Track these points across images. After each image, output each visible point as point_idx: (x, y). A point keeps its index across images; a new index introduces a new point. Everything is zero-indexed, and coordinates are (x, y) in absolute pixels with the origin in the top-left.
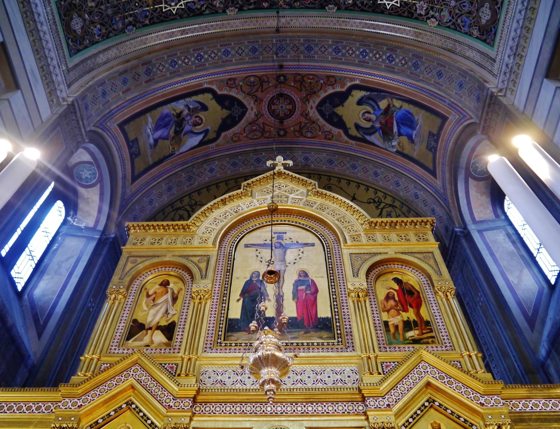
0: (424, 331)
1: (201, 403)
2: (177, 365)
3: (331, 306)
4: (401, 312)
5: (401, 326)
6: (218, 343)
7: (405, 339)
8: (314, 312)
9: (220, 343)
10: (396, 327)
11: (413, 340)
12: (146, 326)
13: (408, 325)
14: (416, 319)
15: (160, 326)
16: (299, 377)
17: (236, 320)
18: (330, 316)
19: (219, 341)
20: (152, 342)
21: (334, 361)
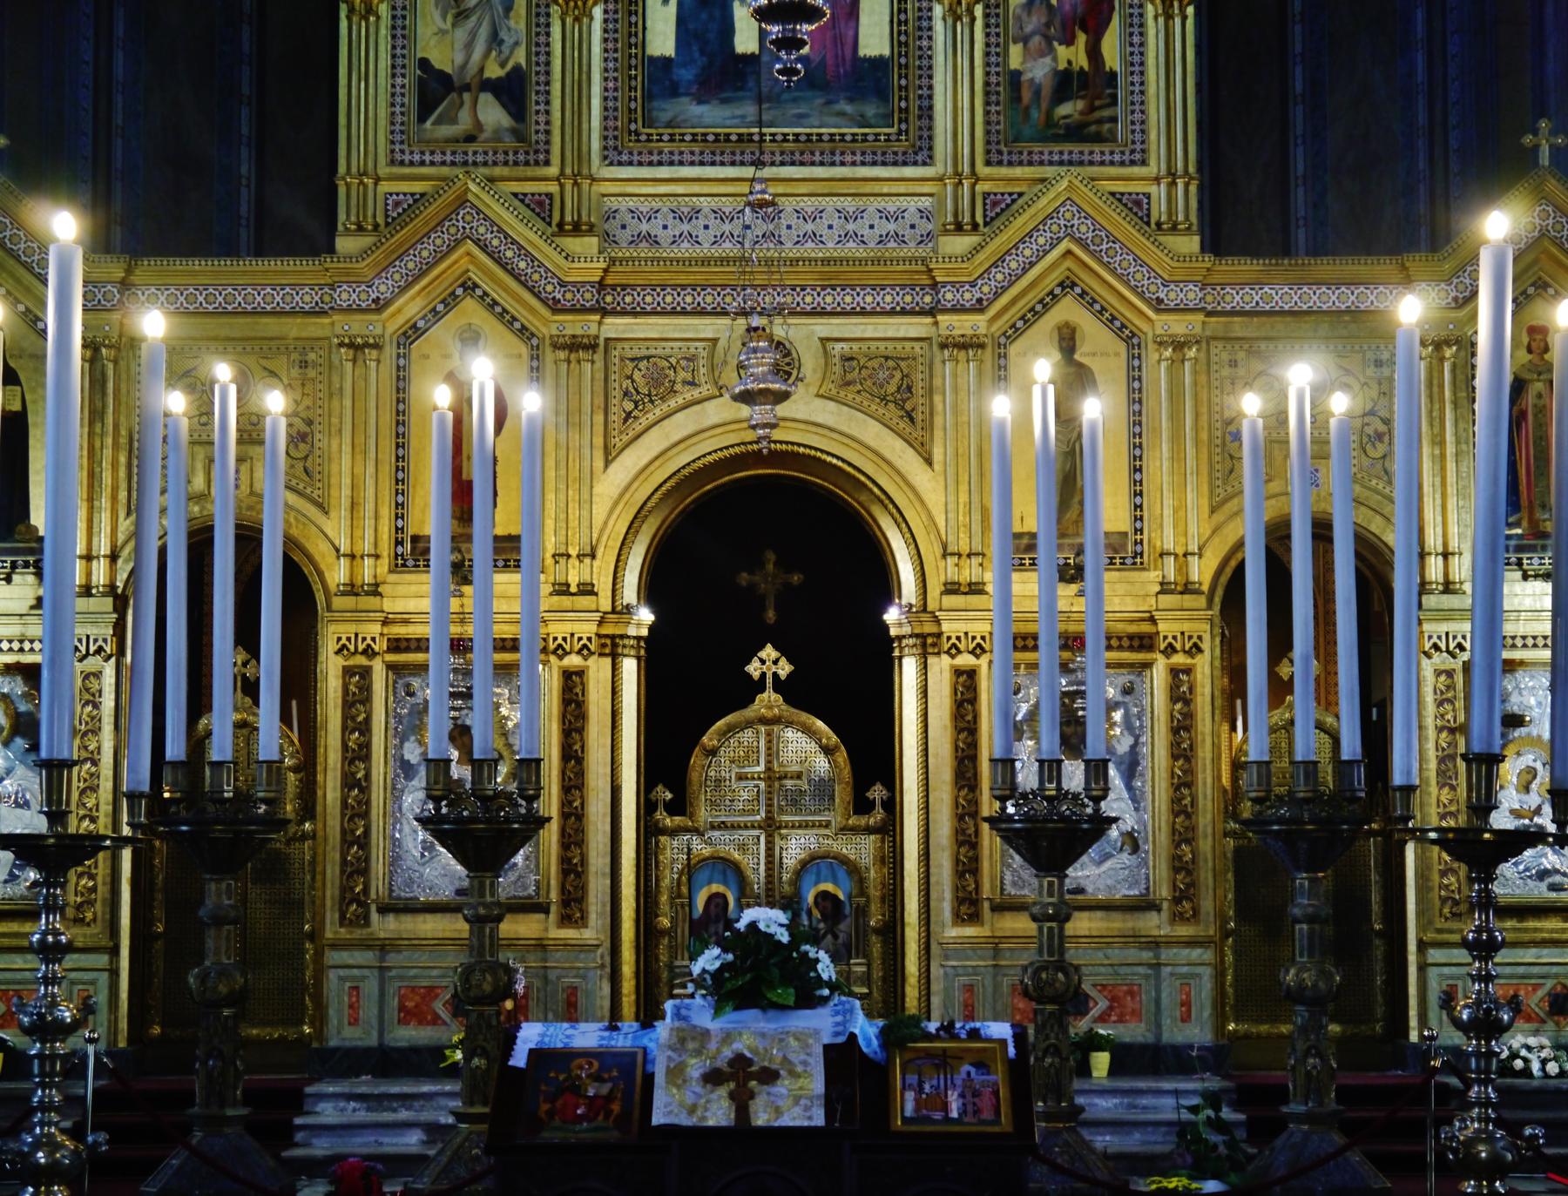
0: (1097, 103)
1: (614, 287)
2: (550, 196)
3: (892, 22)
4: (1056, 44)
5: (1046, 93)
6: (630, 133)
7: (1049, 122)
8: (851, 33)
9: (637, 134)
10: (1037, 93)
11: (1068, 127)
12: (455, 79)
13: (1066, 83)
14: (1086, 67)
15: (489, 80)
16: (810, 227)
17: (665, 62)
18: (886, 52)
19: (633, 127)
20: (478, 125)
21: (885, 190)
